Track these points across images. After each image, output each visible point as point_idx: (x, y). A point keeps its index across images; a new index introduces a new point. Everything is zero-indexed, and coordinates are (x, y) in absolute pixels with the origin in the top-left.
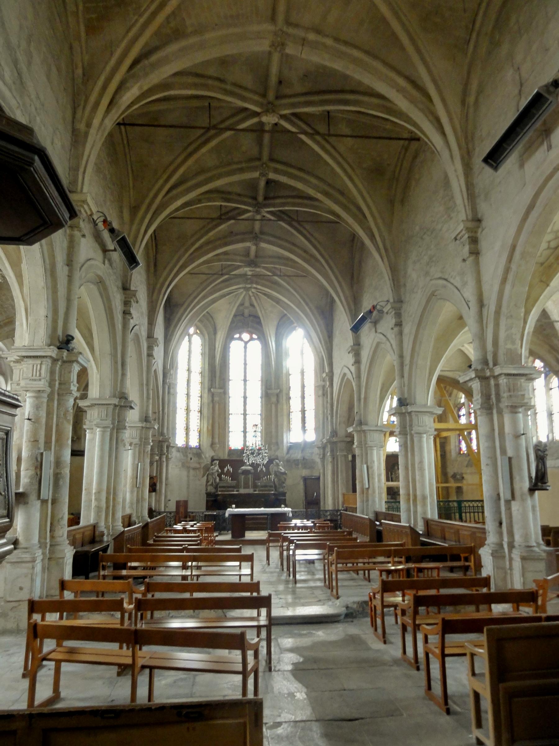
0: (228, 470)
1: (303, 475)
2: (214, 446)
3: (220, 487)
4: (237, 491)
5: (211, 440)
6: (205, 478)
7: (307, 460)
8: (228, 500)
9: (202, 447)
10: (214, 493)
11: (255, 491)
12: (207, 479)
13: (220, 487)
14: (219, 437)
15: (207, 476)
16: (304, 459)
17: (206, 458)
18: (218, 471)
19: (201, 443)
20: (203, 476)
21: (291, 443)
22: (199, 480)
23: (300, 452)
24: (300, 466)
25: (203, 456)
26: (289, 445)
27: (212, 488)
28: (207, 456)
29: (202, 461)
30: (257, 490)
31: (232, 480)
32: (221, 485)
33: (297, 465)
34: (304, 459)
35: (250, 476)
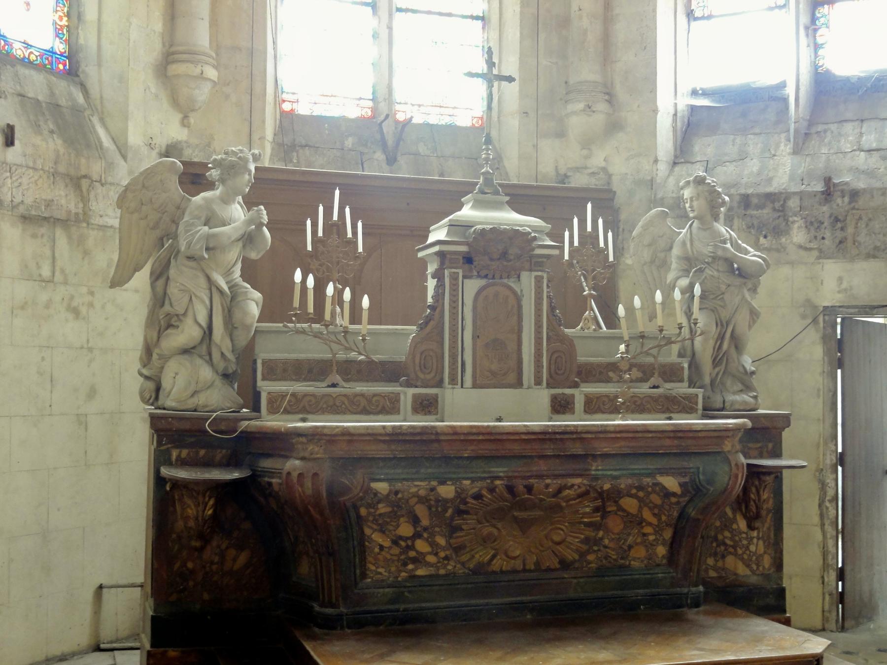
0: (335, 228)
1: (829, 296)
2: (176, 69)
3: (274, 371)
4: (426, 406)
5: (158, 26)
6: (141, 279)
7: (854, 194)
8: (382, 487)
9: (89, 70)
10: (226, 425)
11: (561, 406)
12: (159, 299)
13: (274, 371)
14: (214, 23)
15: (160, 275)
16: (830, 191)
17: (123, 150)
18: (248, 239)
19: (87, 38)
20: (117, 282)
21: (694, 93)
22: (75, 312)
23: (785, 148)
24: (798, 235)
25: (106, 142)
26: (685, 102)
27: (206, 373)
28: (135, 138)
29: (96, 168)
30: (579, 395)
31: (376, 316)
32: (265, 352)
33: (779, 231)
34: (830, 191)
35: (526, 283)
